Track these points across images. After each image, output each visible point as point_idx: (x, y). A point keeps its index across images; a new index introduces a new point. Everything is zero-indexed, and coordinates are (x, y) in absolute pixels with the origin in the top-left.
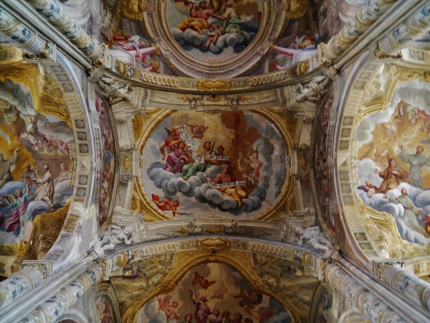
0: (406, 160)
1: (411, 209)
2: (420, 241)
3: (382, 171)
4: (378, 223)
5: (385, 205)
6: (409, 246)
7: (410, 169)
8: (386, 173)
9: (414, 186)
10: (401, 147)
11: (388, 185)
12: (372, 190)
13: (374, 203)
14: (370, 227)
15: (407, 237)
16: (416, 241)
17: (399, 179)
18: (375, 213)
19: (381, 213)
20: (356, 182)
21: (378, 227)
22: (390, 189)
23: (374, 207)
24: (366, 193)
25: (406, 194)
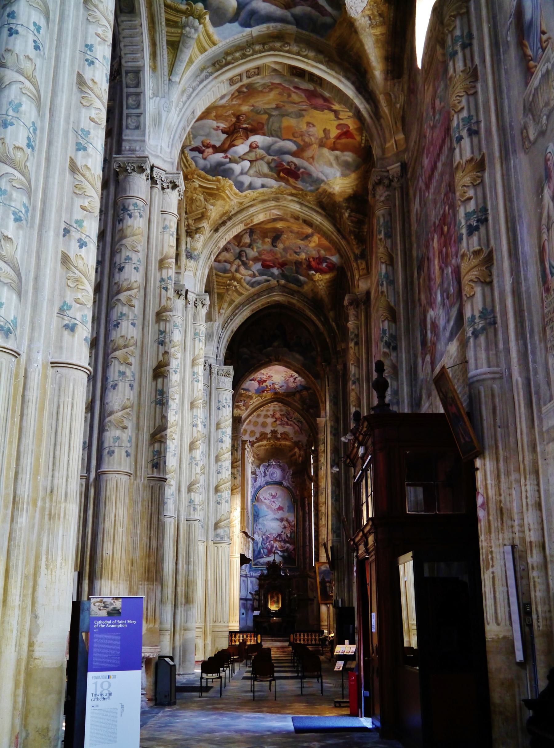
0: (262, 112)
1: (262, 159)
2: (269, 185)
3: (226, 127)
4: (206, 193)
5: (222, 168)
6: (252, 193)
7: (268, 119)
8: (231, 129)
9: (269, 137)
10: (253, 106)
11: (233, 141)
12: (210, 150)
13: (209, 166)
14: (196, 198)
15: (251, 187)
16: (263, 186)
17: (249, 133)
18: (208, 180)
19: (214, 178)
20: (189, 144)
21: (205, 199)
22: (234, 146)
23: (207, 172)
24: (200, 155)
25: (257, 147)
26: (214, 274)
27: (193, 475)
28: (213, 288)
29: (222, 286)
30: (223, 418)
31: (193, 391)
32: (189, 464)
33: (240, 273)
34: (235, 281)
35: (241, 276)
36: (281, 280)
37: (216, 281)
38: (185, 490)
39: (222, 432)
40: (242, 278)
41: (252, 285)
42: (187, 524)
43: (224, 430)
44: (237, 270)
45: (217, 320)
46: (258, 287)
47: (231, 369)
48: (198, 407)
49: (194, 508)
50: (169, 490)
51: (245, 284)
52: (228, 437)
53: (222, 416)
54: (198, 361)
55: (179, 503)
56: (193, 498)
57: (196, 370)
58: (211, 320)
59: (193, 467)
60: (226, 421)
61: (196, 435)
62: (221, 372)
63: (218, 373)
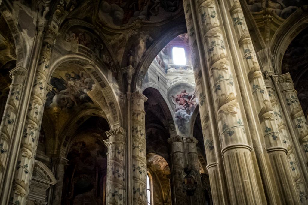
26: (252, 15)
27: (261, 103)
28: (255, 26)
29: (260, 21)
30: (295, 110)
31: (237, 32)
32: (253, 93)
33: (270, 7)
34: (268, 15)
35: (272, 9)
36: (304, 6)
37: (255, 20)
38: (256, 119)
39: (297, 120)
40: (273, 11)
41: (284, 16)
42: (270, 157)
43: (298, 118)
44: (267, 5)
45: (266, 47)
46: (288, 18)
47: (288, 75)
48: (247, 43)
49: (273, 136)
50: (233, 118)
51: (278, 16)
52: (304, 123)
53: (294, 109)
54: (236, 10)
55: (252, 133)
56: (268, 126)
57: (235, 16)
58: (261, 48)
59: (259, 95)
60: (298, 111)
61: (253, 66)
62: (281, 80)
63: (279, 81)
